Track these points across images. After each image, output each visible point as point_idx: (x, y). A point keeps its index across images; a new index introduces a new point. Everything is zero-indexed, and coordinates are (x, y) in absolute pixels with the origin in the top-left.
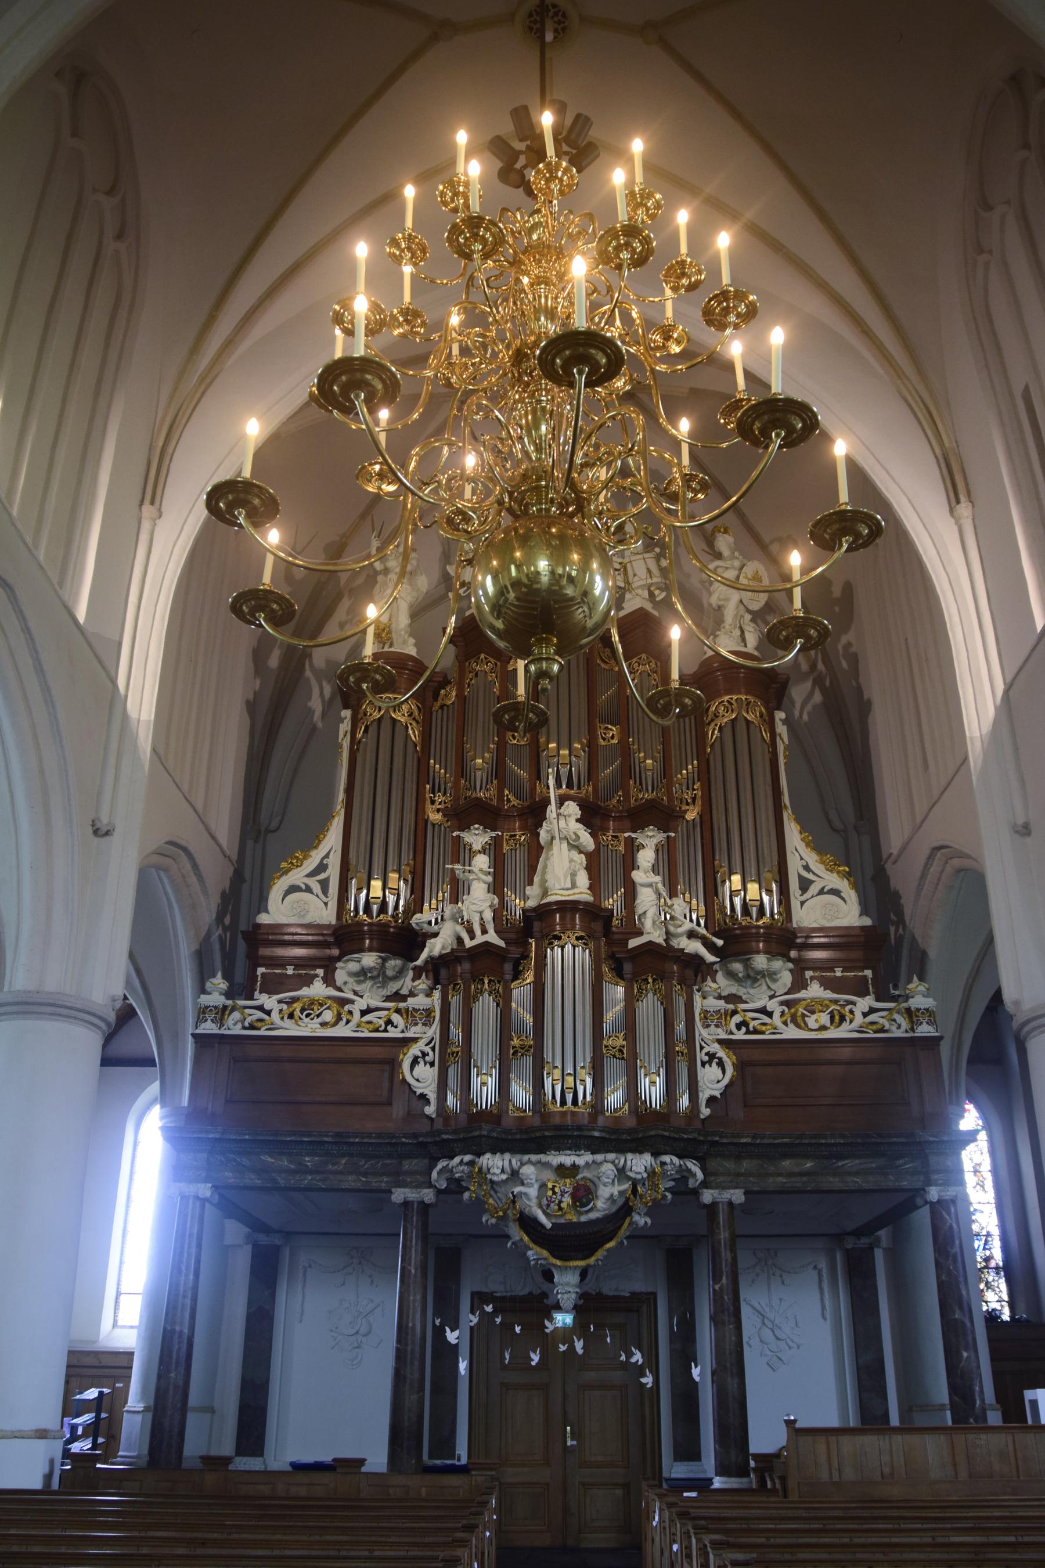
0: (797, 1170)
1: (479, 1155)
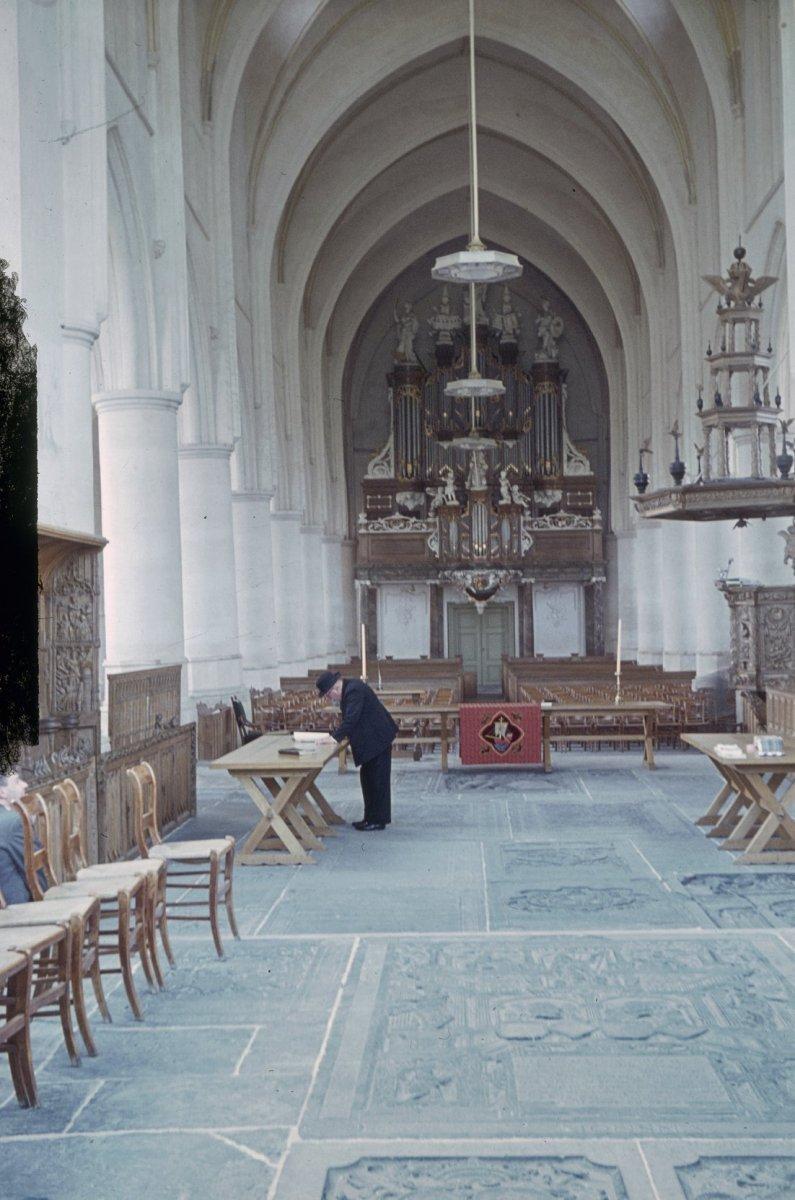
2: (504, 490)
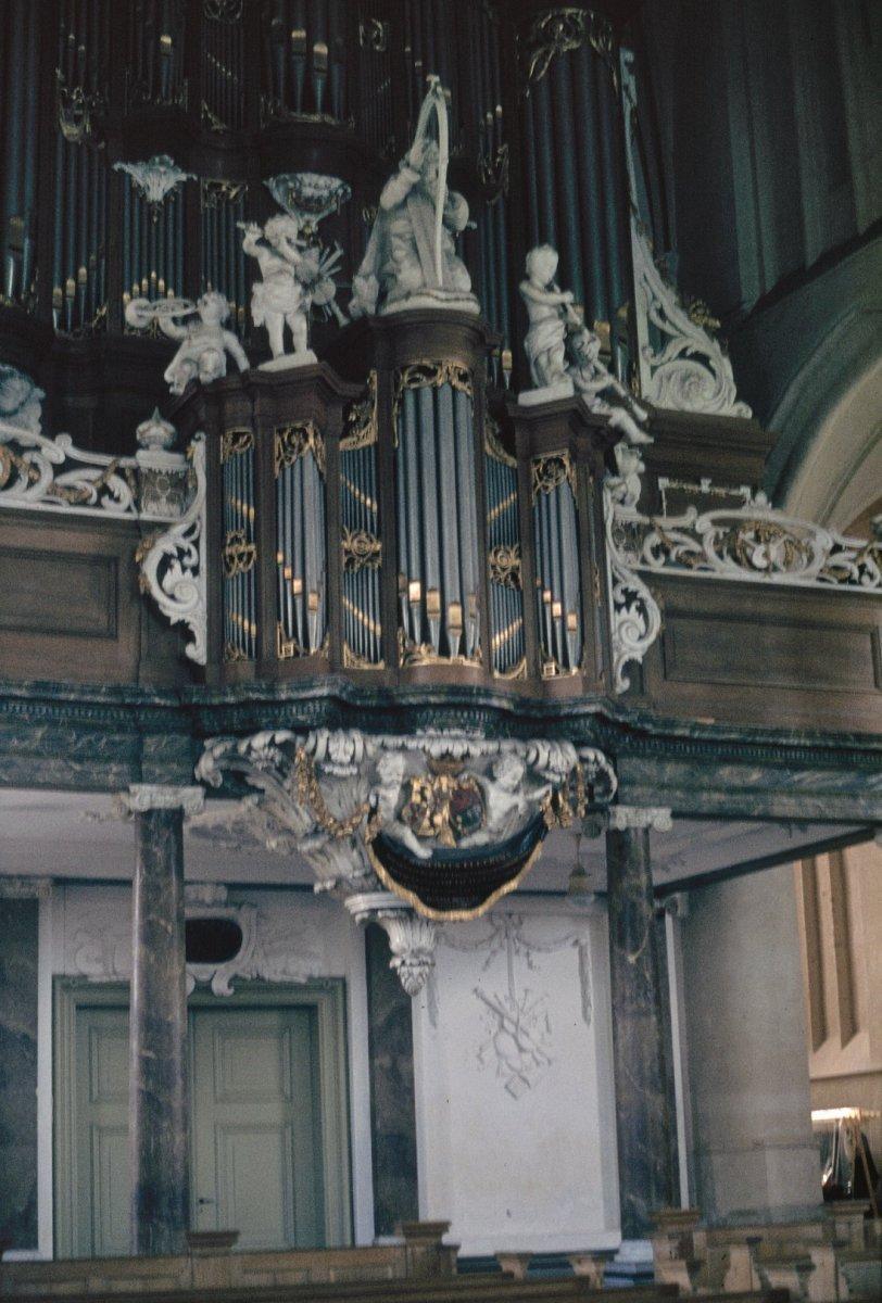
0: (737, 782)
1: (302, 730)
2: (547, 337)
